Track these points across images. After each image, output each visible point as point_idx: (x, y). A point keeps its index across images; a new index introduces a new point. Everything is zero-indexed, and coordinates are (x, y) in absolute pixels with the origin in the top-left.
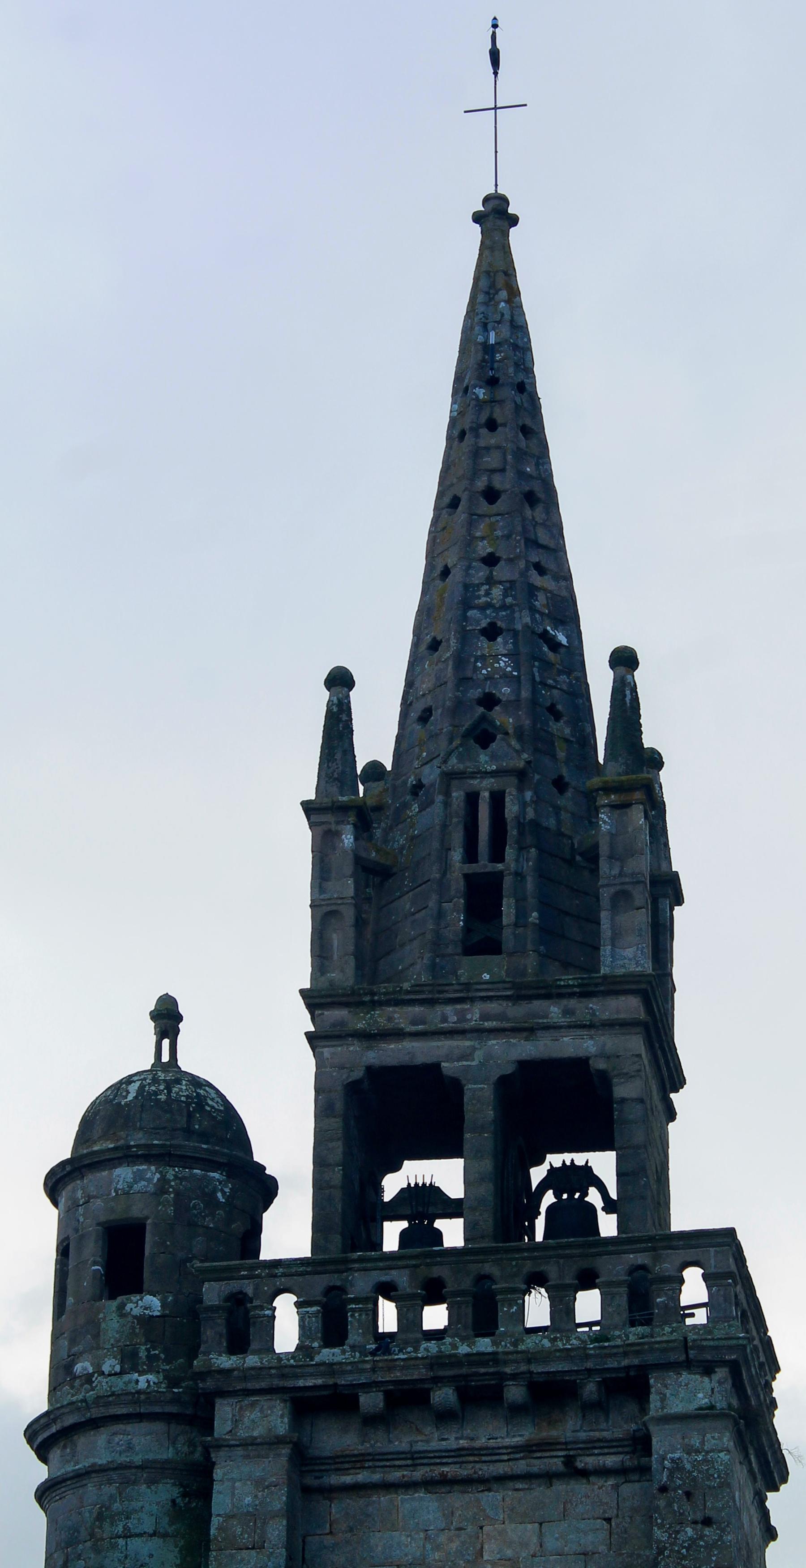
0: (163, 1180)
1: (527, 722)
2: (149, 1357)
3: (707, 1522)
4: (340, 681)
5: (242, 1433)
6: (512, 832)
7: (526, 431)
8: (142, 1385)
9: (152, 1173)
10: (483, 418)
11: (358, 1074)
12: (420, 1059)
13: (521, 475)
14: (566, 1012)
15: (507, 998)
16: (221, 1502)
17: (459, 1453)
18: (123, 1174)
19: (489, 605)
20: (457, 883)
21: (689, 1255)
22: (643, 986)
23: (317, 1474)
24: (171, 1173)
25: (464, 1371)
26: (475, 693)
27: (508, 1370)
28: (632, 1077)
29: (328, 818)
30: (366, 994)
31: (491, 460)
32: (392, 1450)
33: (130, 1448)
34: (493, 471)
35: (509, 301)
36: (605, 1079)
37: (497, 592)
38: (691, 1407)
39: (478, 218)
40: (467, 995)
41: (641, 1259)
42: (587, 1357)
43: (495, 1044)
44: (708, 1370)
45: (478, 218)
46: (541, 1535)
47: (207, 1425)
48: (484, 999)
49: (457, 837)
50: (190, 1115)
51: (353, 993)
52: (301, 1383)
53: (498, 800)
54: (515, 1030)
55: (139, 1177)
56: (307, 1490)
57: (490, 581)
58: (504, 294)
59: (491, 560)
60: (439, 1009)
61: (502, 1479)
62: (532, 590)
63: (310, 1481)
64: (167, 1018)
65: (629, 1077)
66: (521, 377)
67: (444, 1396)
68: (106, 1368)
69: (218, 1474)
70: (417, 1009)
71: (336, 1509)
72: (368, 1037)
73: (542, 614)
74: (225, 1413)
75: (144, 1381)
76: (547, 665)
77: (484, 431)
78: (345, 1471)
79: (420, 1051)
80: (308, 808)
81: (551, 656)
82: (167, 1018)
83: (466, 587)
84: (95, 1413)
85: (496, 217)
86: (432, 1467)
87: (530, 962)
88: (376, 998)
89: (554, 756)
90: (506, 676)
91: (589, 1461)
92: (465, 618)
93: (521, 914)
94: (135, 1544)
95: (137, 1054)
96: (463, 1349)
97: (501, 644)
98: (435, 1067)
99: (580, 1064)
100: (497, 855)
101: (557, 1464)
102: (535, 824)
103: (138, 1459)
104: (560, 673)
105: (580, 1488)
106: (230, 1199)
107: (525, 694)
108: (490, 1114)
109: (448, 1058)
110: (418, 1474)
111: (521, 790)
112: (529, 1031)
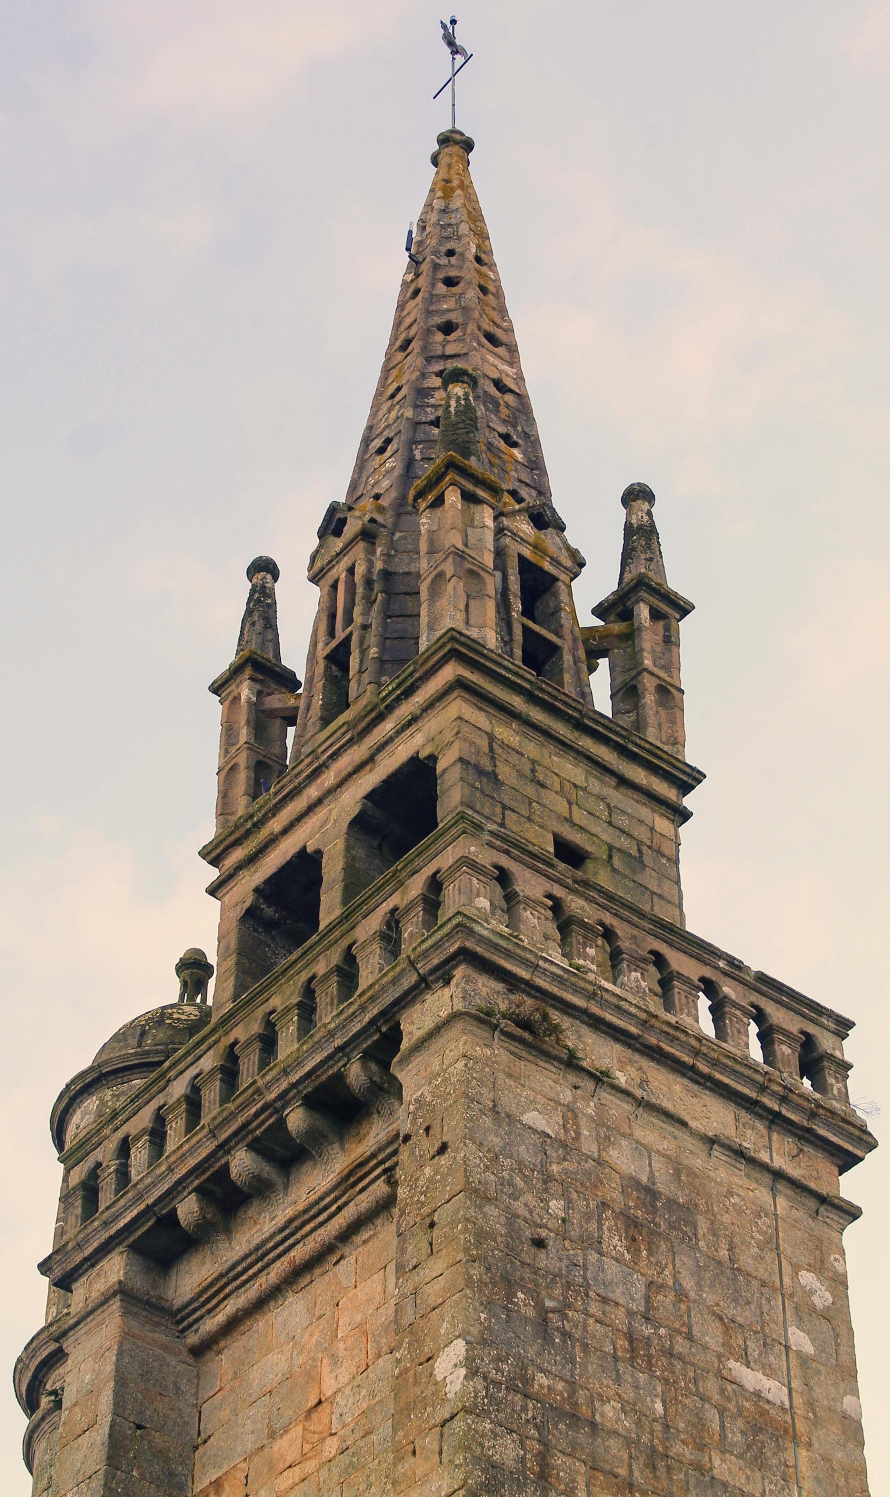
4: (264, 569)
22: (449, 647)
23: (195, 1327)
28: (453, 742)
30: (246, 821)
32: (235, 1258)
63: (193, 1339)
85: (455, 145)
86: (282, 1259)
88: (255, 819)
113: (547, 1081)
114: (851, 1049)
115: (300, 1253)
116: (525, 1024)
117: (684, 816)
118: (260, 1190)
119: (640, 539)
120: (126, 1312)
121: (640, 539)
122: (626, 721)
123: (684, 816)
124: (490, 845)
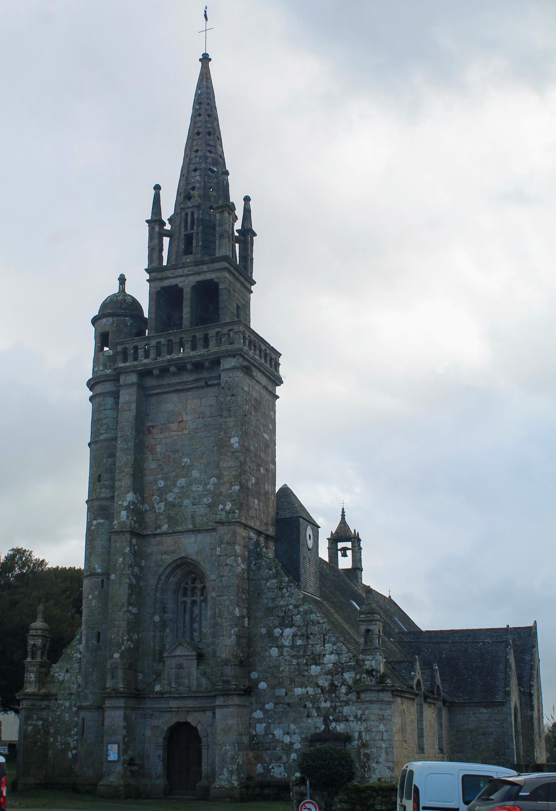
0: (113, 321)
1: (202, 193)
2: (110, 366)
3: (233, 395)
4: (157, 188)
5: (126, 382)
6: (196, 222)
7: (209, 116)
8: (108, 372)
9: (111, 319)
10: (197, 114)
11: (159, 289)
12: (174, 284)
13: (206, 127)
14: (208, 268)
15: (193, 265)
16: (121, 400)
17: (180, 383)
18: (104, 320)
19: (195, 163)
20: (182, 236)
21: (231, 327)
24: (115, 319)
25: (176, 362)
26: (190, 187)
27: (186, 361)
29: (153, 224)
31: (198, 125)
33: (105, 388)
34: (199, 127)
35: (206, 82)
36: (216, 285)
37: (197, 159)
38: (230, 367)
39: (200, 60)
40: (184, 266)
41: (219, 330)
42: (204, 356)
43: (191, 278)
44: (234, 356)
45: (200, 60)
46: (201, 402)
47: (118, 380)
48: (188, 266)
49: (183, 225)
50: (121, 304)
51: (157, 268)
52: (138, 369)
53: (193, 214)
54: (196, 274)
55: (108, 321)
56: (146, 395)
57: (196, 157)
58: (205, 80)
59: (197, 151)
60: (178, 270)
61: (191, 389)
62: (207, 158)
63: (146, 393)
64: (122, 280)
65: (223, 283)
66: (209, 101)
67: (173, 369)
68: (100, 369)
69: (121, 393)
70: (173, 271)
71: (153, 400)
72: (161, 279)
73: (209, 164)
74: (122, 378)
75: (108, 371)
76: (210, 177)
77: (198, 117)
78: (154, 390)
79: (173, 282)
80: (147, 221)
81: (211, 174)
82: (122, 280)
83: (190, 159)
84: (97, 380)
85: (205, 59)
87: (199, 256)
89: (210, 201)
90: (198, 181)
91: (210, 383)
92: (189, 167)
93: (197, 243)
94: (106, 412)
95: (115, 289)
96: (176, 357)
97: (198, 173)
98: (177, 285)
99: (211, 280)
100: (192, 228)
101: (203, 384)
102: (202, 220)
103: (106, 391)
104: (214, 178)
105: (210, 389)
106: (131, 324)
107: (202, 185)
108: (189, 296)
109: (180, 283)
110: (171, 389)
111: (199, 210)
112: (199, 274)
113: (247, 380)
116: (245, 367)
118: (174, 374)
121: (247, 212)
123: (252, 292)
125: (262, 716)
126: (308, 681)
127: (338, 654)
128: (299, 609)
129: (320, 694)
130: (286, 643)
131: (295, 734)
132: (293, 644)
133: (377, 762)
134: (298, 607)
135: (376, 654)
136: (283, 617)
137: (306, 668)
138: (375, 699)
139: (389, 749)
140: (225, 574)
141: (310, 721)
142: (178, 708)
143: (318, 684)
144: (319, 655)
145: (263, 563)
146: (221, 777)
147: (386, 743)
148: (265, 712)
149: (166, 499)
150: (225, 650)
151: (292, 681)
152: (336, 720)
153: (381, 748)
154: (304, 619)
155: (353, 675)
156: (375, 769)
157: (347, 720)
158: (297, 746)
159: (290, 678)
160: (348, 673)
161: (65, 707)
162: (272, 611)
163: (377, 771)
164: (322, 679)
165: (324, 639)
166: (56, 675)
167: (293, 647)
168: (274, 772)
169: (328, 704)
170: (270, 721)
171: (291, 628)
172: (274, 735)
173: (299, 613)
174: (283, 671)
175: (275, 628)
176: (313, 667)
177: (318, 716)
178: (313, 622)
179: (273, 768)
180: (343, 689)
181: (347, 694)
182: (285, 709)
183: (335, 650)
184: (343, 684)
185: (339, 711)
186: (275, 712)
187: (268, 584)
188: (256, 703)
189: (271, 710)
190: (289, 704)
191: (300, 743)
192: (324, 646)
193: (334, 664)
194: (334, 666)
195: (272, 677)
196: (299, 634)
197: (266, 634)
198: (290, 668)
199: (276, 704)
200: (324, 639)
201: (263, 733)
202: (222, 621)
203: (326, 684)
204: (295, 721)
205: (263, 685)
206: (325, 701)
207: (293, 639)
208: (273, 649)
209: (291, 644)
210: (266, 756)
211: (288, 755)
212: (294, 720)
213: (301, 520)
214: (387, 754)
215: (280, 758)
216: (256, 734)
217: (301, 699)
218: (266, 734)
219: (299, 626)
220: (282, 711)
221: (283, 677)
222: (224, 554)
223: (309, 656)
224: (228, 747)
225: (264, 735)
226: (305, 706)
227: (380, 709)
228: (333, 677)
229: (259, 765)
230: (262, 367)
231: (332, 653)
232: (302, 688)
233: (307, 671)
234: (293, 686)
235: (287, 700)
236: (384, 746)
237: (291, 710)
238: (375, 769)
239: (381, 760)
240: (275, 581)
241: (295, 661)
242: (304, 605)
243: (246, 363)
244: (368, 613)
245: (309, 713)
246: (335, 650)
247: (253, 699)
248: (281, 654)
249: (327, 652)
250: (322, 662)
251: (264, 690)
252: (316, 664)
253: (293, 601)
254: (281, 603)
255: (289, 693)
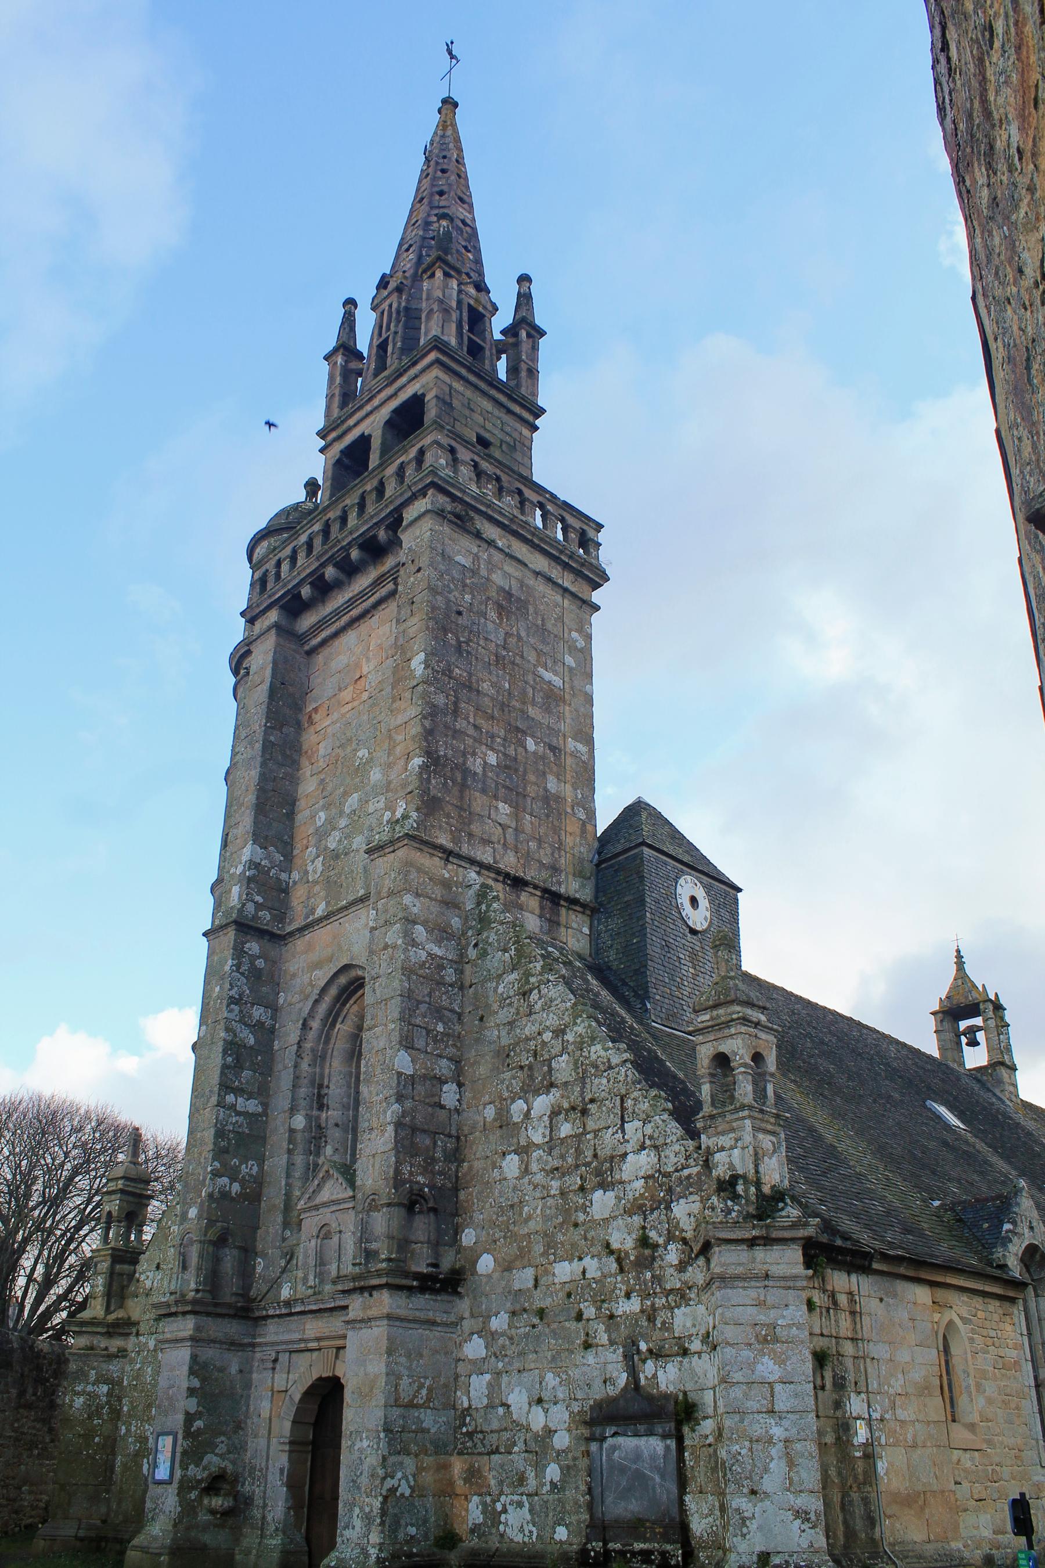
17: (352, 602)
63: (307, 648)
71: (320, 658)
85: (449, 104)
114: (601, 537)
115: (355, 613)
116: (458, 516)
117: (536, 428)
118: (337, 585)
119: (524, 300)
120: (278, 635)
121: (524, 300)
122: (512, 383)
123: (536, 428)
124: (447, 435)
125: (483, 1353)
126: (586, 1239)
127: (656, 1147)
128: (566, 1038)
129: (615, 1276)
130: (537, 1138)
131: (555, 1404)
132: (551, 1139)
133: (753, 1492)
134: (563, 1032)
135: (742, 1128)
136: (530, 1067)
137: (581, 1201)
138: (740, 1270)
139: (798, 1446)
140: (381, 973)
141: (590, 1358)
142: (318, 1339)
143: (608, 1245)
144: (612, 1157)
145: (493, 938)
146: (347, 1533)
147: (786, 1423)
148: (490, 1337)
149: (326, 848)
150: (373, 1166)
151: (550, 1245)
152: (655, 1354)
153: (770, 1441)
154: (576, 1063)
155: (696, 1207)
156: (744, 1520)
157: (685, 1352)
158: (562, 1440)
159: (546, 1235)
160: (682, 1201)
161: (148, 1351)
162: (508, 1056)
163: (753, 1525)
164: (618, 1229)
165: (623, 1109)
166: (143, 1277)
167: (551, 1145)
168: (506, 1524)
169: (634, 1305)
170: (500, 1365)
171: (548, 1093)
172: (509, 1406)
173: (564, 1050)
174: (529, 1217)
175: (513, 1101)
176: (598, 1194)
177: (612, 1343)
178: (596, 1067)
179: (505, 1511)
180: (673, 1255)
181: (682, 1267)
182: (534, 1326)
183: (651, 1138)
184: (670, 1238)
185: (664, 1323)
186: (511, 1338)
187: (500, 990)
188: (472, 1316)
189: (503, 1334)
190: (541, 1313)
191: (569, 1430)
192: (623, 1132)
193: (646, 1178)
194: (646, 1187)
195: (505, 1237)
196: (566, 1105)
197: (495, 1120)
198: (544, 1206)
199: (514, 1313)
200: (623, 1109)
201: (485, 1401)
202: (370, 1092)
203: (629, 1244)
204: (556, 1364)
205: (486, 1263)
206: (628, 1296)
207: (551, 1122)
208: (509, 1157)
209: (546, 1140)
210: (492, 1470)
211: (540, 1468)
212: (554, 1358)
213: (646, 850)
214: (791, 1464)
215: (522, 1479)
216: (470, 1407)
217: (569, 1295)
218: (491, 1406)
219: (566, 1084)
220: (527, 1335)
221: (529, 1235)
222: (382, 922)
223: (587, 1164)
224: (365, 1443)
225: (487, 1407)
226: (579, 1317)
227: (760, 1304)
228: (645, 1219)
229: (476, 1499)
230: (523, 528)
231: (643, 1147)
232: (571, 1261)
233: (584, 1209)
234: (552, 1257)
235: (540, 1300)
236: (777, 1432)
237: (547, 1330)
238: (744, 1520)
239: (769, 1483)
240: (514, 976)
241: (555, 1184)
242: (575, 1024)
243: (459, 508)
244: (715, 1006)
245: (587, 1334)
246: (651, 1138)
247: (464, 1306)
248: (526, 1171)
249: (629, 1148)
250: (617, 1177)
251: (489, 1276)
252: (604, 1186)
253: (552, 1020)
254: (527, 1032)
255: (543, 1281)
